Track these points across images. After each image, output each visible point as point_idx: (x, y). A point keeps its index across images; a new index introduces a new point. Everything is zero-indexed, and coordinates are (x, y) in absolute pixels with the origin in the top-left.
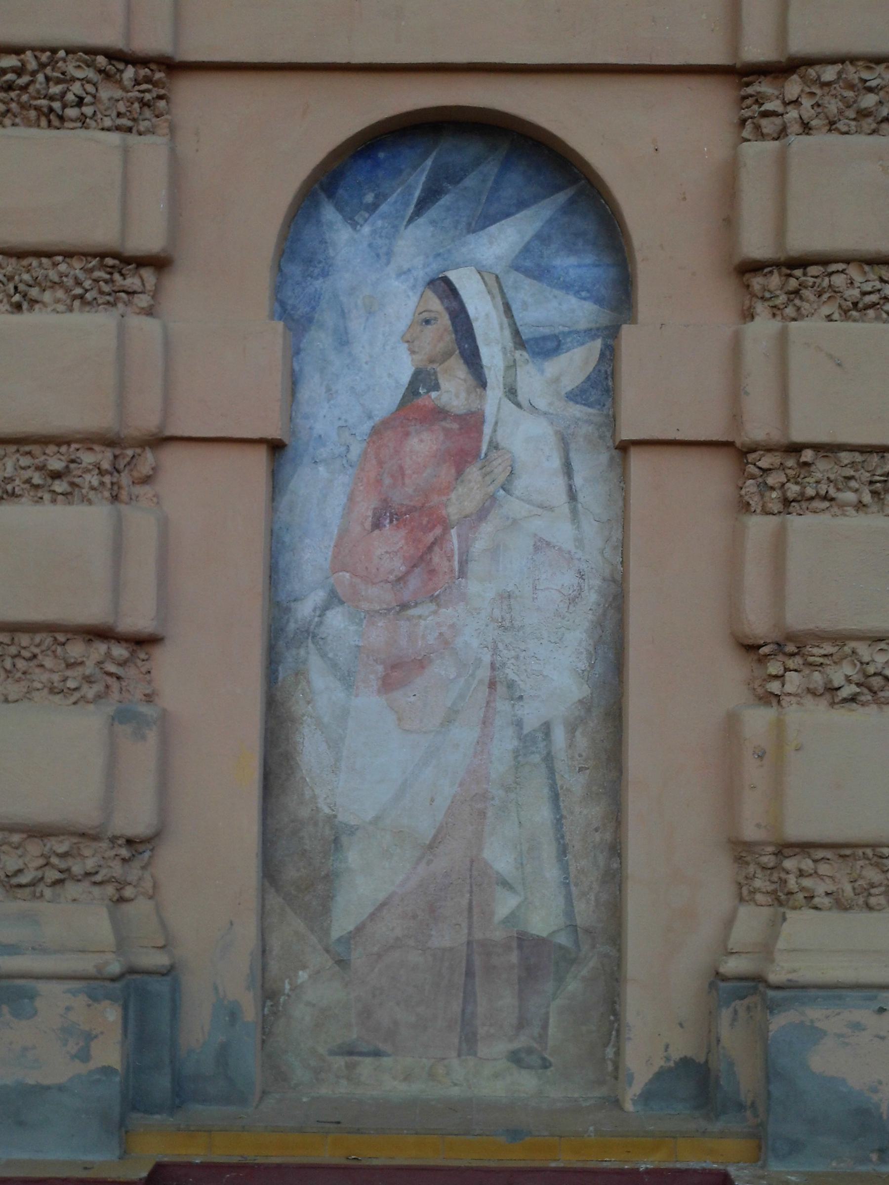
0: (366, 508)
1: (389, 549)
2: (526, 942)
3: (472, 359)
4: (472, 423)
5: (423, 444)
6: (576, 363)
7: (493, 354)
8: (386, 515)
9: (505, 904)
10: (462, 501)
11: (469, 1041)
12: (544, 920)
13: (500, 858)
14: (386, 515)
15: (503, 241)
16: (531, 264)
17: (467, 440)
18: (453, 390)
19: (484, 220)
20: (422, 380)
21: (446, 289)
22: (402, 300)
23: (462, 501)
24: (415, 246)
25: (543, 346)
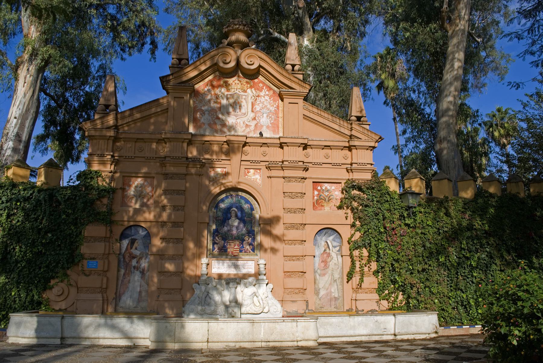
0: (321, 261)
1: (323, 265)
2: (335, 298)
3: (329, 248)
4: (329, 253)
5: (325, 255)
6: (338, 248)
7: (331, 248)
8: (322, 262)
9: (333, 294)
10: (328, 260)
11: (331, 306)
12: (336, 296)
13: (333, 291)
14: (322, 262)
15: (331, 238)
16: (334, 240)
17: (329, 255)
18: (328, 251)
19: (330, 236)
20: (325, 250)
21: (327, 242)
22: (323, 243)
23: (328, 260)
24: (324, 238)
25: (335, 247)
